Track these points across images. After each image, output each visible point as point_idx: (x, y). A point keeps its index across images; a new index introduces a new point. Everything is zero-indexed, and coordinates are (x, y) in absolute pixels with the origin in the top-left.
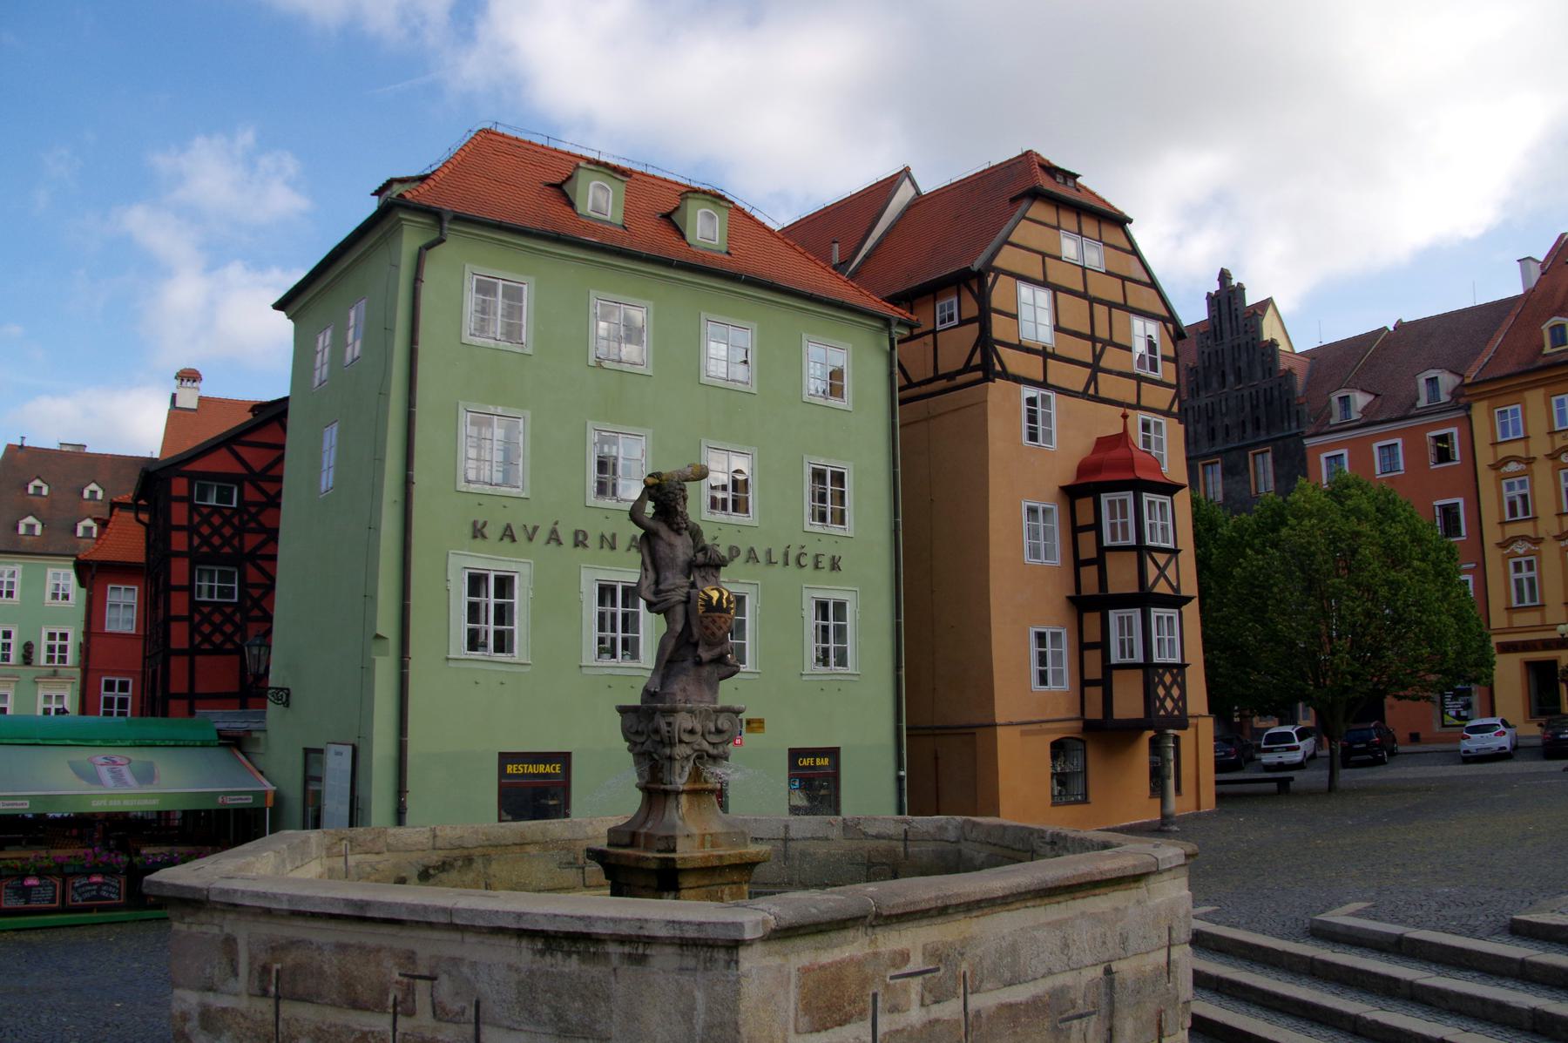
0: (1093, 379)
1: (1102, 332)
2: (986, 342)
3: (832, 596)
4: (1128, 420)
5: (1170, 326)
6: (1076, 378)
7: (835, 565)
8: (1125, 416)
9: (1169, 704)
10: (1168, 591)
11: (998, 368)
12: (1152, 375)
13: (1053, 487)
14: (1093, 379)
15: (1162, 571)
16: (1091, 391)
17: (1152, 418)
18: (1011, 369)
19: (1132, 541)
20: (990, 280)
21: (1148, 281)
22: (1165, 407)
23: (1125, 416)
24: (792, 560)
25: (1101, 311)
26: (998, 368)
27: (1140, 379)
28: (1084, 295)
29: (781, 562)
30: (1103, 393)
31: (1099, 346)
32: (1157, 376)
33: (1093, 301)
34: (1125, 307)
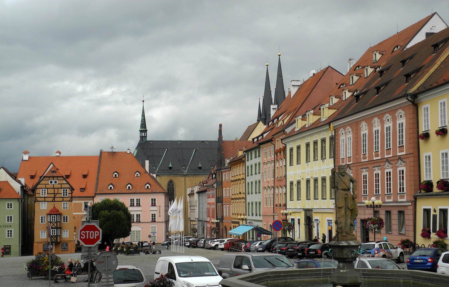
1: (56, 192)
2: (36, 198)
3: (10, 230)
4: (55, 205)
5: (71, 189)
6: (51, 199)
7: (10, 226)
8: (54, 205)
10: (55, 227)
11: (36, 200)
13: (46, 214)
14: (54, 199)
15: (54, 224)
16: (54, 201)
17: (65, 202)
18: (38, 200)
19: (49, 221)
20: (36, 190)
21: (66, 183)
22: (69, 200)
23: (54, 205)
24: (4, 226)
25: (56, 190)
26: (36, 200)
29: (2, 227)
30: (55, 201)
31: (55, 194)
32: (67, 196)
33: (54, 188)
34: (61, 188)
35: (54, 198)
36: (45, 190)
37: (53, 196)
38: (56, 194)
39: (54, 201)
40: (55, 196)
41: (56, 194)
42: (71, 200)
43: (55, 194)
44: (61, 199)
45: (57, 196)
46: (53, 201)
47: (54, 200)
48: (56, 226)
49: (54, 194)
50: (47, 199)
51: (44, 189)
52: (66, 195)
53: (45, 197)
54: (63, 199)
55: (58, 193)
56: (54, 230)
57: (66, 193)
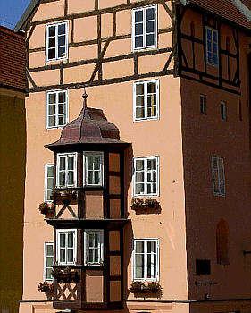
0: (98, 68)
9: (67, 293)
10: (72, 218)
12: (150, 48)
14: (98, 68)
16: (96, 78)
17: (146, 82)
27: (136, 56)
28: (97, 12)
31: (103, 44)
35: (99, 62)
36: (62, 29)
37: (92, 52)
38: (109, 40)
39: (96, 78)
40: (101, 53)
41: (109, 40)
42: (171, 66)
43: (103, 44)
44: (126, 68)
45: (114, 49)
46: (97, 83)
47: (100, 76)
48: (76, 214)
49: (98, 41)
50: (71, 75)
51: (57, 25)
52: (150, 41)
53: (62, 66)
54: (136, 71)
55: (114, 37)
56: (66, 231)
57: (150, 27)
